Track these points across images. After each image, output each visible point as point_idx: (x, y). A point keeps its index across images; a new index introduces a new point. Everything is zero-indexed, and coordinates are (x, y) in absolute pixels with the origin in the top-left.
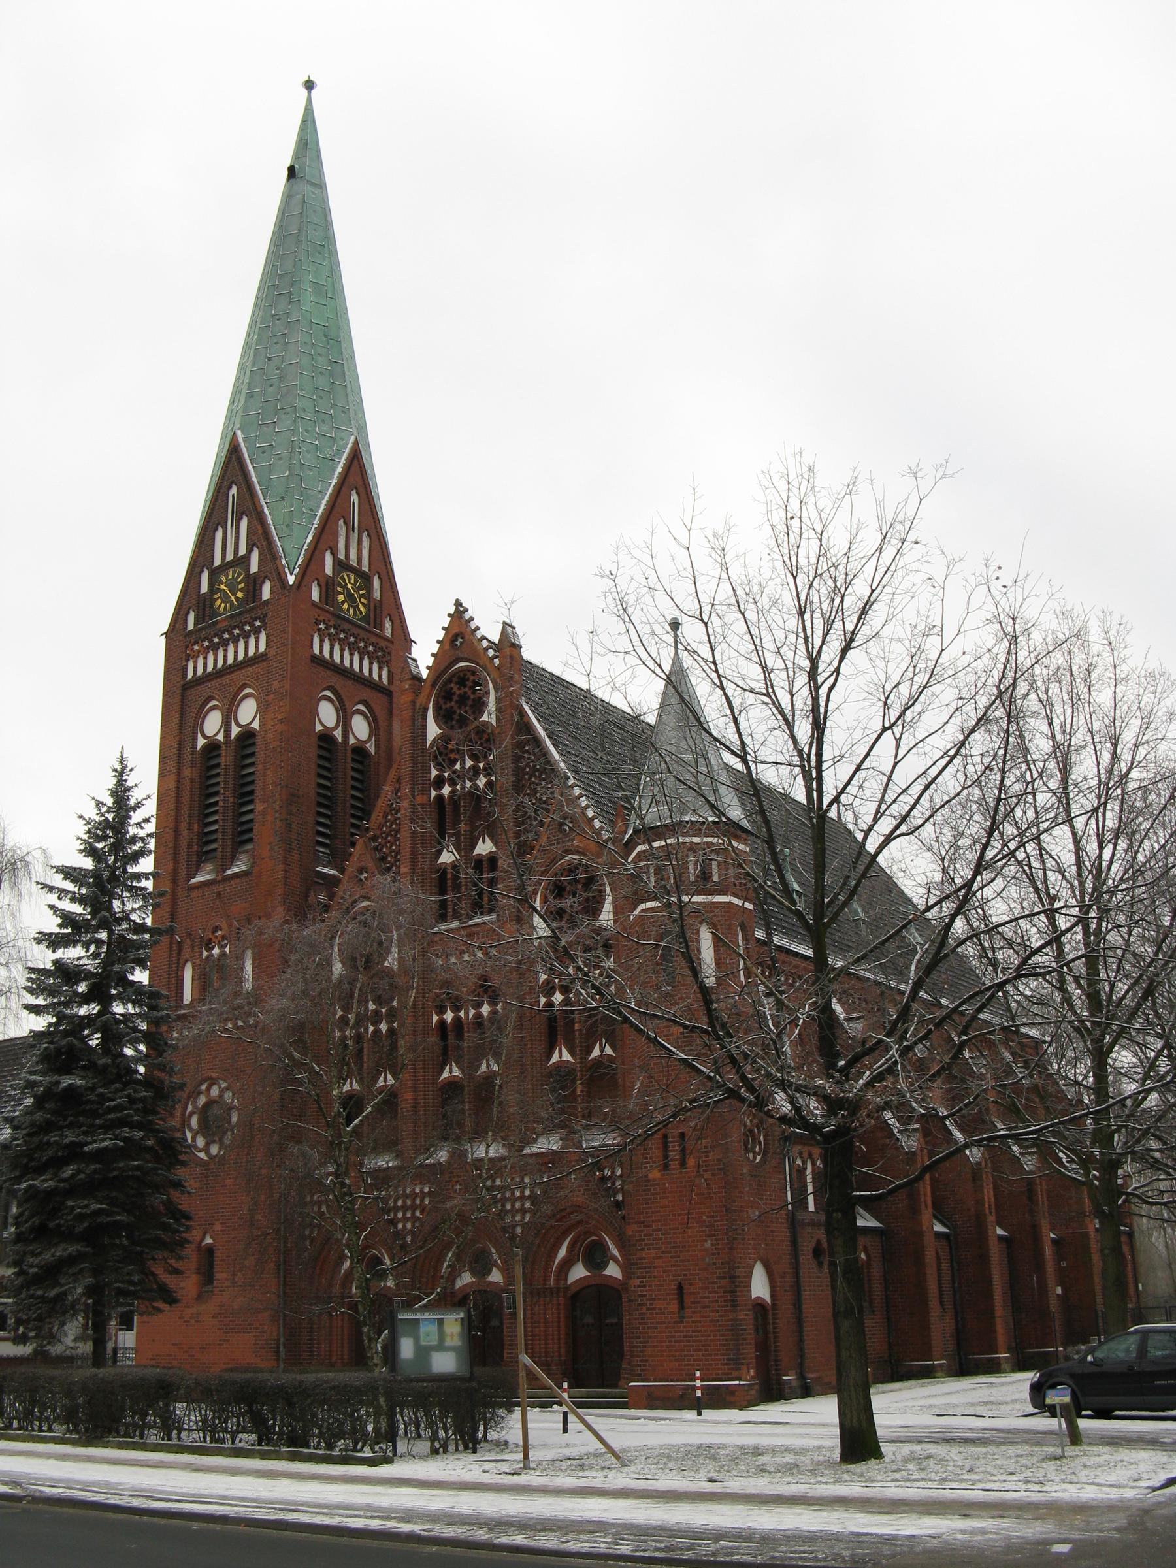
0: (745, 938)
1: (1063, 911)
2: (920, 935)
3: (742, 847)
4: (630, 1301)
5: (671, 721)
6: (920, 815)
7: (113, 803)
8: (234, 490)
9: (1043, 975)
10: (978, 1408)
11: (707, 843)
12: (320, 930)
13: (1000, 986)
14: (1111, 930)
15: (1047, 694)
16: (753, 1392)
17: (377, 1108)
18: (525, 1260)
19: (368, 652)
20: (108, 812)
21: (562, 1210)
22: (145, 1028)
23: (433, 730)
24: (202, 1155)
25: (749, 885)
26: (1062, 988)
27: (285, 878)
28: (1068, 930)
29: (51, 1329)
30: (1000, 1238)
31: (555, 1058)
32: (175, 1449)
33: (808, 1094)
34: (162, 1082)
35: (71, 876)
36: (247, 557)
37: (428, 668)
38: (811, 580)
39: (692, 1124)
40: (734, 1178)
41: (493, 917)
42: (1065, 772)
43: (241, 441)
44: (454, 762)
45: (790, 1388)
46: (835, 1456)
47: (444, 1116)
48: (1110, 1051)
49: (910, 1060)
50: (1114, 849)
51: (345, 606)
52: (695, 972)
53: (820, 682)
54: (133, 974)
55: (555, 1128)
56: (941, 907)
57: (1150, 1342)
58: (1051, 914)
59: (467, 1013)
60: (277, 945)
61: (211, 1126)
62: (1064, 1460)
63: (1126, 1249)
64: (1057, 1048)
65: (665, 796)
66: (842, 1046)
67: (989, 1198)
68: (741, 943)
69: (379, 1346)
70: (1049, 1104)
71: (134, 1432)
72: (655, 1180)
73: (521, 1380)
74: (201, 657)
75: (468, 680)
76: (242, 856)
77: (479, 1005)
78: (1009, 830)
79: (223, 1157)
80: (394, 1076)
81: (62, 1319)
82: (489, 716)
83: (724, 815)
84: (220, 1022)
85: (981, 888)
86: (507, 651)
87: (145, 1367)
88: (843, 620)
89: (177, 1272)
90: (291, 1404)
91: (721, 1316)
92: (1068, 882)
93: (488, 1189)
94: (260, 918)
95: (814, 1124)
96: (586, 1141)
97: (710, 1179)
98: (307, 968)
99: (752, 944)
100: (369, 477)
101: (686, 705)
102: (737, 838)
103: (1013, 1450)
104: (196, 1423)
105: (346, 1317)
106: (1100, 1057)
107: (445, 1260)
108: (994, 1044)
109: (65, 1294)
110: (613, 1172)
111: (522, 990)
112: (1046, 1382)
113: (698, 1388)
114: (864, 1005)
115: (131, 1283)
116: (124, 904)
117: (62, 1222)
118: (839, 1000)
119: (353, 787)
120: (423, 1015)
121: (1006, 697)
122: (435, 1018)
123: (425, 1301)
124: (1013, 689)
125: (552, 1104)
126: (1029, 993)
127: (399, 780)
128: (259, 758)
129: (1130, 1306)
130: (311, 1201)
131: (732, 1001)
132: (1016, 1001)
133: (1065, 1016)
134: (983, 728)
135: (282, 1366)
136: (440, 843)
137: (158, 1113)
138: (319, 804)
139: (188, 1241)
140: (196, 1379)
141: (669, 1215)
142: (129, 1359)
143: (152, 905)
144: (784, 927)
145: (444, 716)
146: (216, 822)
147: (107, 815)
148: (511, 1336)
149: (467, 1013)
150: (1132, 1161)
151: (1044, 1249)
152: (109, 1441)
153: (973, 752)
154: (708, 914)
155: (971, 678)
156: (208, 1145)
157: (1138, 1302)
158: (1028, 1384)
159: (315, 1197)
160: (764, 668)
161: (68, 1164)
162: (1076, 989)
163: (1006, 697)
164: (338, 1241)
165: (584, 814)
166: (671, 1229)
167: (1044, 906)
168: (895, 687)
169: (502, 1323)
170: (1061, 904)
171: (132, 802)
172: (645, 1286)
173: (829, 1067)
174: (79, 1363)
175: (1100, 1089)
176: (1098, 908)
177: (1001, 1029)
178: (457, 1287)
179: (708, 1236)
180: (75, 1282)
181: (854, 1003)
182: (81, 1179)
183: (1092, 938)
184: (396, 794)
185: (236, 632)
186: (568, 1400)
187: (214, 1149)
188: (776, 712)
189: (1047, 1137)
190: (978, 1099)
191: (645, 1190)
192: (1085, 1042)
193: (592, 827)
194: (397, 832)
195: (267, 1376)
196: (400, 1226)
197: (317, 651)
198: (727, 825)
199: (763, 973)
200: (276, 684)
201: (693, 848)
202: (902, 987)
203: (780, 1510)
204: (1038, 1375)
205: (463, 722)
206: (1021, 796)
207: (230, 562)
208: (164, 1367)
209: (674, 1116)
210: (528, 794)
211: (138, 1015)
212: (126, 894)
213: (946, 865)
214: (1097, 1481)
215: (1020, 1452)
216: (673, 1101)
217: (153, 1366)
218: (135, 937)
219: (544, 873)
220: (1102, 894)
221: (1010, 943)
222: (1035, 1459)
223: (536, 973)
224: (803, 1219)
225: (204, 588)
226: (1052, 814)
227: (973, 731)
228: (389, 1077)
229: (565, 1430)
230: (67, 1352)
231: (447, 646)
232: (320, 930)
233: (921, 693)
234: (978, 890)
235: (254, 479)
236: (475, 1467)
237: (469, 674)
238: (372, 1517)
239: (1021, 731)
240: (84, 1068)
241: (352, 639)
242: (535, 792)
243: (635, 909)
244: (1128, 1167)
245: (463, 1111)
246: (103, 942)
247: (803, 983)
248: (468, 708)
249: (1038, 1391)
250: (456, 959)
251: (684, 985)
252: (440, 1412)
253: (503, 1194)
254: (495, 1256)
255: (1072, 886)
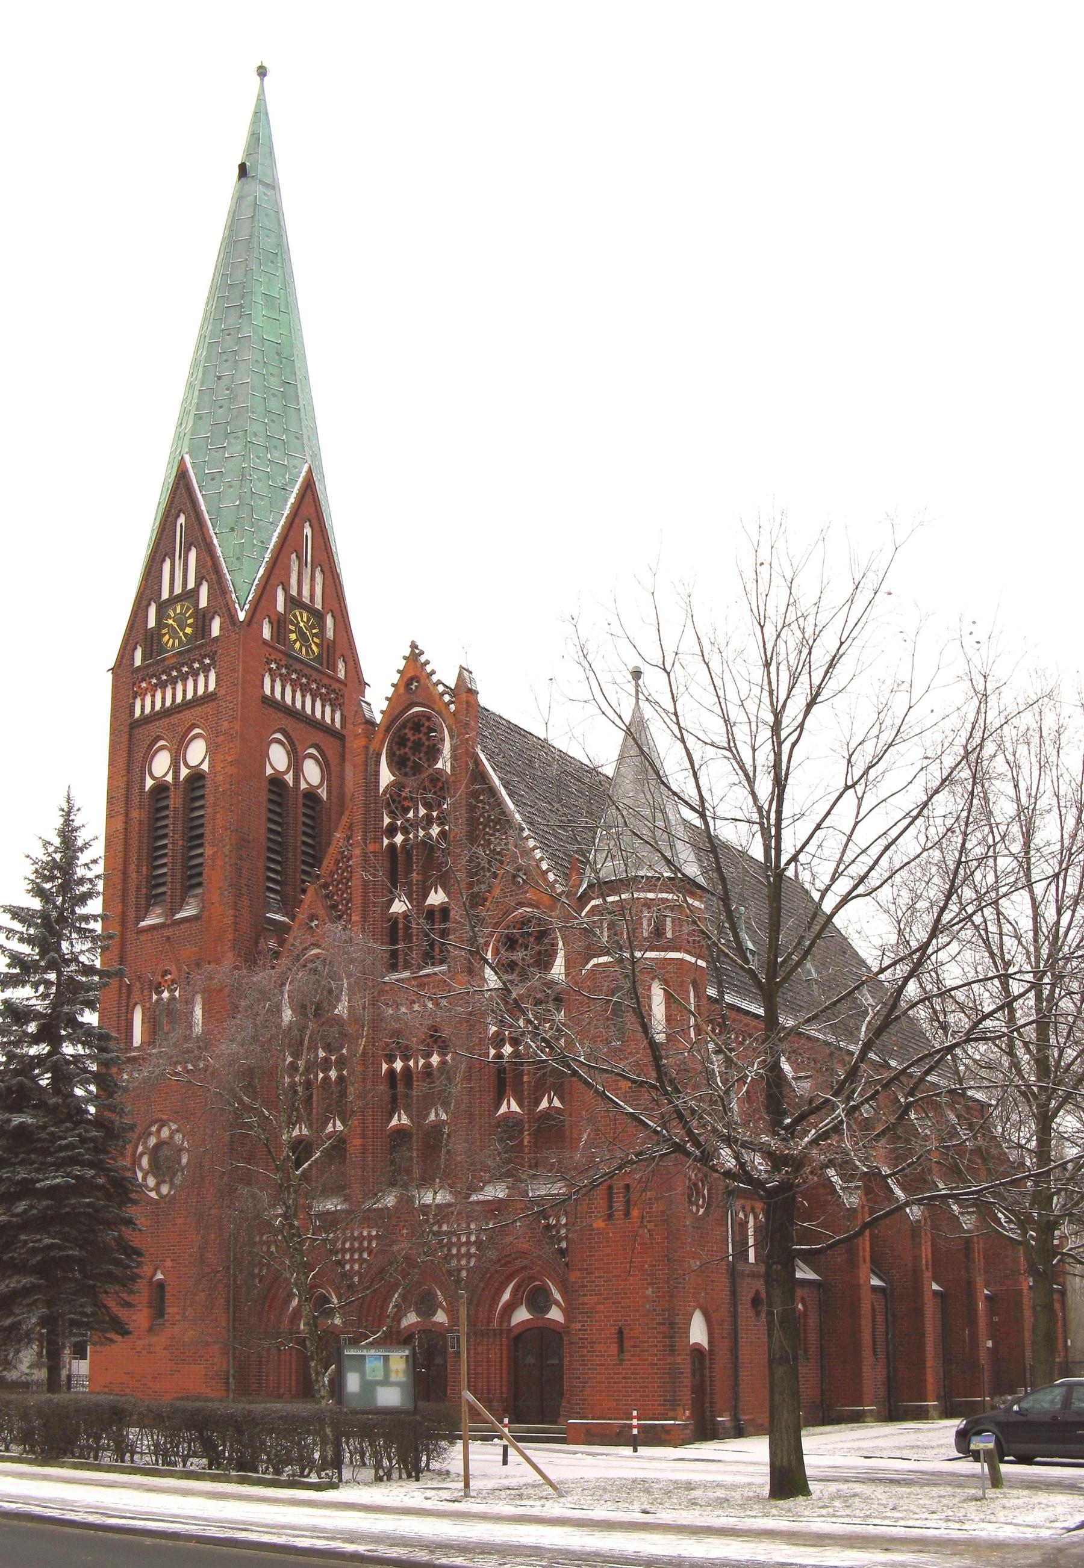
0: (697, 996)
1: (1017, 976)
2: (872, 997)
3: (697, 904)
4: (572, 1343)
5: (629, 772)
6: (879, 877)
7: (61, 844)
8: (182, 520)
9: (993, 1039)
10: (904, 1452)
11: (662, 899)
12: (271, 976)
13: (950, 1049)
14: (1064, 996)
15: (1014, 755)
16: (688, 1431)
17: (326, 1153)
18: (470, 1302)
19: (321, 694)
20: (55, 852)
21: (506, 1256)
22: (95, 1069)
23: (386, 777)
24: (153, 1194)
25: (703, 943)
26: (1011, 1053)
27: (235, 923)
28: (1021, 995)
29: (7, 1356)
30: (935, 1293)
31: (503, 1109)
32: (128, 1470)
33: (754, 1150)
34: (112, 1122)
35: (19, 916)
36: (196, 591)
37: (382, 712)
38: (779, 630)
39: (637, 1176)
40: (678, 1230)
41: (444, 968)
42: (1028, 837)
43: (189, 466)
44: (407, 810)
45: (724, 1428)
46: (765, 1492)
47: (393, 1162)
48: (1055, 1115)
49: (855, 1119)
50: (1073, 916)
51: (298, 645)
52: (646, 1028)
53: (783, 738)
54: (82, 1016)
55: (502, 1177)
56: (895, 969)
57: (1075, 1395)
58: (1005, 979)
59: (416, 1063)
60: (227, 991)
61: (161, 1167)
62: (984, 1501)
63: (1057, 1306)
64: (1002, 1111)
65: (621, 850)
66: (789, 1104)
67: (926, 1255)
68: (692, 1001)
69: (326, 1379)
70: (991, 1165)
71: (89, 1454)
72: (598, 1229)
73: (463, 1415)
74: (149, 694)
75: (423, 725)
76: (191, 900)
77: (428, 1055)
78: (968, 893)
79: (174, 1197)
80: (343, 1122)
81: (17, 1347)
82: (444, 763)
83: (680, 871)
84: (170, 1065)
85: (936, 952)
86: (464, 697)
87: (98, 1393)
88: (810, 673)
89: (129, 1305)
90: (240, 1432)
91: (658, 1360)
92: (1024, 948)
93: (434, 1234)
94: (209, 963)
95: (758, 1179)
96: (532, 1190)
97: (653, 1230)
98: (257, 1014)
99: (704, 1002)
100: (323, 508)
101: (645, 757)
102: (692, 894)
103: (936, 1491)
104: (149, 1446)
105: (294, 1352)
106: (1045, 1121)
107: (391, 1300)
108: (940, 1105)
109: (19, 1323)
110: (558, 1221)
111: (471, 1042)
112: (971, 1429)
113: (635, 1427)
114: (812, 1064)
115: (84, 1314)
116: (72, 946)
117: (16, 1255)
118: (788, 1059)
119: (305, 834)
120: (373, 1063)
121: (972, 757)
122: (385, 1067)
123: (371, 1339)
124: (981, 750)
125: (499, 1154)
126: (978, 1057)
127: (351, 827)
128: (209, 801)
129: (1057, 1360)
130: (261, 1241)
131: (681, 1057)
132: (964, 1064)
133: (1012, 1081)
134: (947, 789)
135: (231, 1396)
136: (391, 892)
137: (108, 1153)
138: (270, 850)
139: (140, 1277)
140: (148, 1406)
141: (612, 1263)
142: (83, 1386)
143: (100, 947)
144: (736, 986)
145: (398, 763)
146: (165, 865)
147: (54, 855)
148: (455, 1374)
149: (416, 1063)
150: (1069, 1222)
151: (977, 1304)
152: (64, 1462)
153: (936, 814)
154: (664, 972)
155: (939, 737)
156: (158, 1184)
157: (1066, 1356)
158: (955, 1429)
159: (264, 1238)
160: (727, 721)
161: (20, 1199)
162: (1025, 1054)
163: (972, 757)
164: (287, 1280)
165: (538, 867)
166: (613, 1276)
167: (998, 971)
168: (860, 744)
169: (445, 1361)
170: (1016, 969)
171: (80, 843)
172: (586, 1330)
173: (775, 1125)
174: (35, 1388)
175: (1043, 1153)
176: (1053, 975)
177: (948, 1092)
178: (403, 1326)
179: (648, 1284)
180: (29, 1312)
181: (803, 1062)
182: (34, 1214)
183: (1044, 1004)
184: (348, 842)
185: (185, 669)
186: (509, 1434)
187: (165, 1189)
188: (736, 766)
189: (987, 1197)
190: (922, 1159)
191: (589, 1239)
192: (1030, 1106)
193: (546, 880)
194: (348, 880)
195: (217, 1405)
196: (348, 1267)
197: (268, 692)
198: (683, 881)
199: (713, 1030)
200: (225, 725)
201: (648, 904)
202: (852, 1048)
203: (707, 1540)
204: (964, 1422)
205: (417, 769)
206: (981, 860)
207: (178, 596)
208: (117, 1395)
209: (620, 1168)
210: (482, 845)
211: (89, 1056)
212: (74, 935)
213: (902, 927)
214: (1014, 1521)
215: (942, 1493)
216: (619, 1154)
217: (106, 1393)
218: (84, 979)
219: (496, 925)
220: (1057, 961)
221: (962, 1007)
222: (957, 1500)
223: (486, 1025)
224: (743, 1271)
225: (152, 623)
226: (1012, 879)
227: (936, 792)
228: (338, 1123)
229: (505, 1462)
230: (23, 1378)
231: (402, 690)
232: (271, 976)
233: (886, 751)
234: (933, 954)
235: (203, 508)
236: (417, 1494)
237: (424, 720)
238: (318, 1537)
239: (985, 793)
240: (35, 1106)
241: (304, 680)
242: (489, 842)
243: (587, 963)
244: (1065, 1228)
245: (411, 1158)
246: (52, 983)
247: (753, 1041)
248: (422, 755)
249: (963, 1438)
250: (407, 1009)
251: (634, 1040)
252: (385, 1442)
253: (449, 1239)
254: (441, 1298)
255: (1028, 952)
